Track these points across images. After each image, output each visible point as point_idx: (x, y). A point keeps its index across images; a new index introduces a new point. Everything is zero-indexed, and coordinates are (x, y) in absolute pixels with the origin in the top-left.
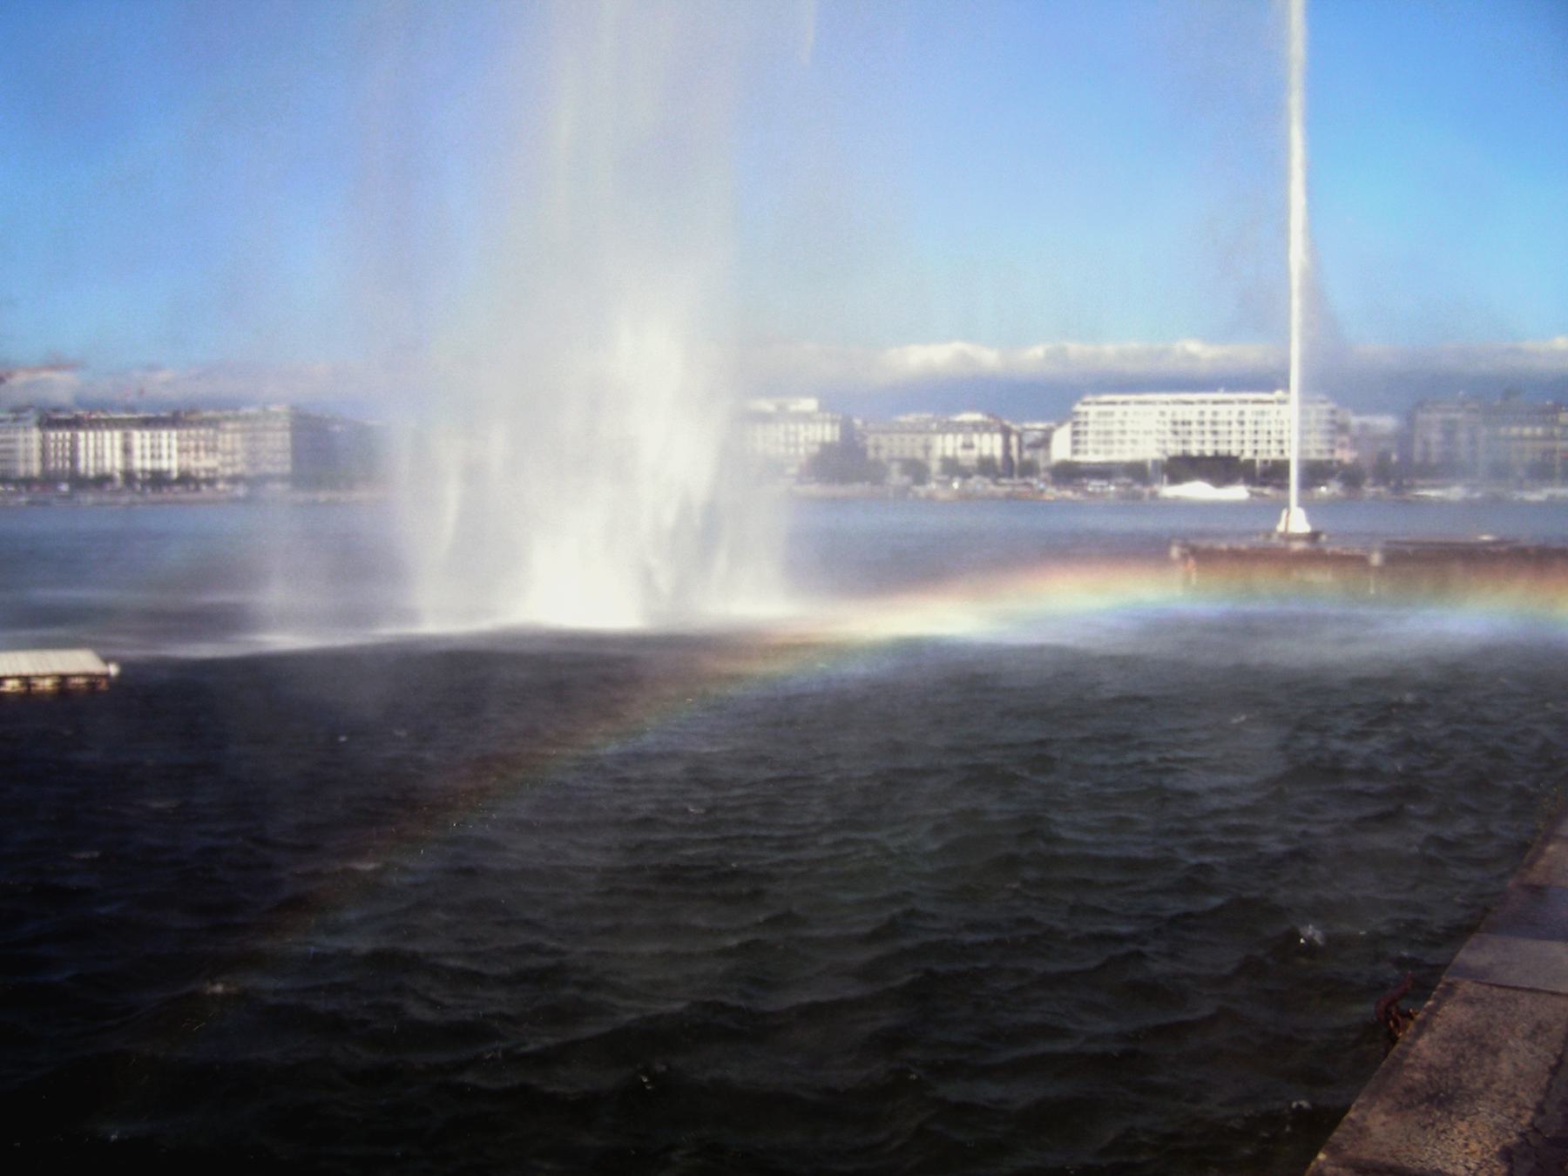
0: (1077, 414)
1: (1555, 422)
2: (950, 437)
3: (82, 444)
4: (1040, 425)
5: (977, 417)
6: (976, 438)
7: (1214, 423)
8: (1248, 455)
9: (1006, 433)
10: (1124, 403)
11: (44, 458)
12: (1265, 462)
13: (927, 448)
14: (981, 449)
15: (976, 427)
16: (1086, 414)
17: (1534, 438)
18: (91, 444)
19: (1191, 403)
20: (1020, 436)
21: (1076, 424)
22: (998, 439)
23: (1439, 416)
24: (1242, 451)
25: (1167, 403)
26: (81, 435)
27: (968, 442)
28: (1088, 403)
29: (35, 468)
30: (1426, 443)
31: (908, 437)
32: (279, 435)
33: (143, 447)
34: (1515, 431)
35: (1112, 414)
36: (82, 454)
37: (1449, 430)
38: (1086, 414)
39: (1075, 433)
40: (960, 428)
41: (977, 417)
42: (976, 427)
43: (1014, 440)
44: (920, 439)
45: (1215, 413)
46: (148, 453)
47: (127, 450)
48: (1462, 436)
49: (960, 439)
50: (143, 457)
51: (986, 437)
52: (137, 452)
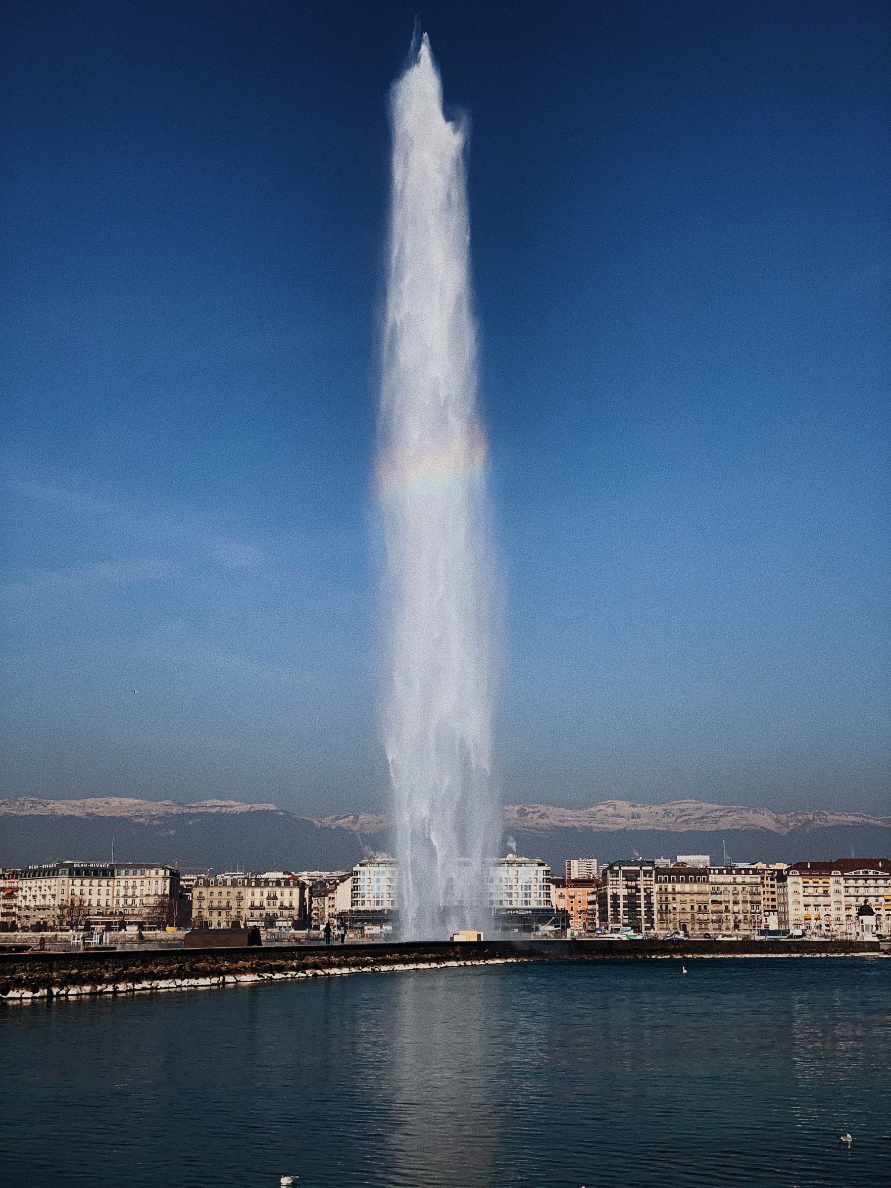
1: (705, 881)
2: (257, 891)
5: (280, 875)
6: (278, 891)
15: (278, 883)
16: (364, 873)
22: (296, 891)
38: (364, 873)
40: (267, 882)
42: (278, 883)
44: (234, 892)
49: (266, 891)
51: (287, 891)
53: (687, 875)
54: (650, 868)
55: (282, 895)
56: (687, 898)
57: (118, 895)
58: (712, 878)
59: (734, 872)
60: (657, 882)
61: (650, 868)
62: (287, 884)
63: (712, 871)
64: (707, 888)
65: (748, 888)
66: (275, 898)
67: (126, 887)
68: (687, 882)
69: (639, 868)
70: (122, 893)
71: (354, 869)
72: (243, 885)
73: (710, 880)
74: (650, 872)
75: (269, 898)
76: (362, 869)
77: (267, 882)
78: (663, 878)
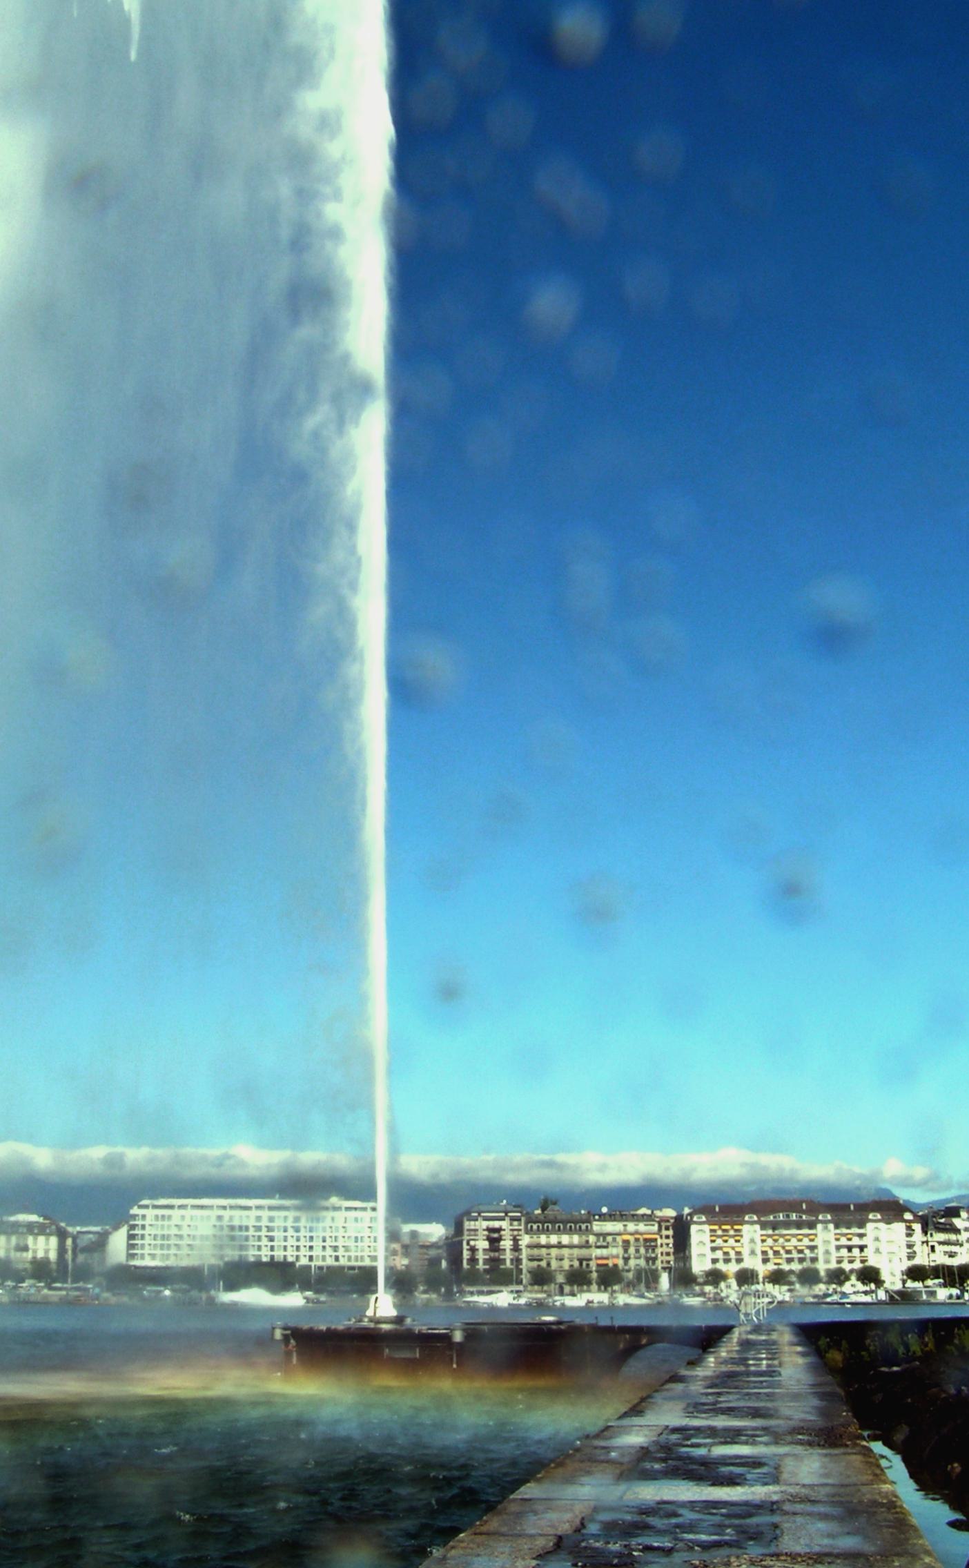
0: (134, 1217)
1: (588, 1231)
4: (97, 1229)
5: (34, 1218)
7: (269, 1229)
8: (304, 1261)
9: (62, 1235)
10: (180, 1207)
12: (321, 1268)
14: (35, 1251)
15: (31, 1228)
16: (144, 1217)
17: (571, 1246)
19: (210, 1207)
20: (75, 1239)
21: (133, 1227)
22: (54, 1241)
23: (485, 1224)
24: (298, 1257)
25: (224, 1208)
27: (22, 1244)
28: (146, 1207)
30: (473, 1250)
34: (554, 1239)
35: (170, 1217)
37: (494, 1239)
38: (144, 1217)
39: (131, 1237)
41: (34, 1218)
42: (31, 1228)
43: (69, 1242)
45: (271, 1219)
48: (507, 1244)
49: (14, 1240)
51: (41, 1239)
56: (566, 1252)
60: (527, 1233)
66: (26, 1249)
69: (503, 1214)
74: (518, 1219)
77: (16, 1225)
78: (535, 1227)
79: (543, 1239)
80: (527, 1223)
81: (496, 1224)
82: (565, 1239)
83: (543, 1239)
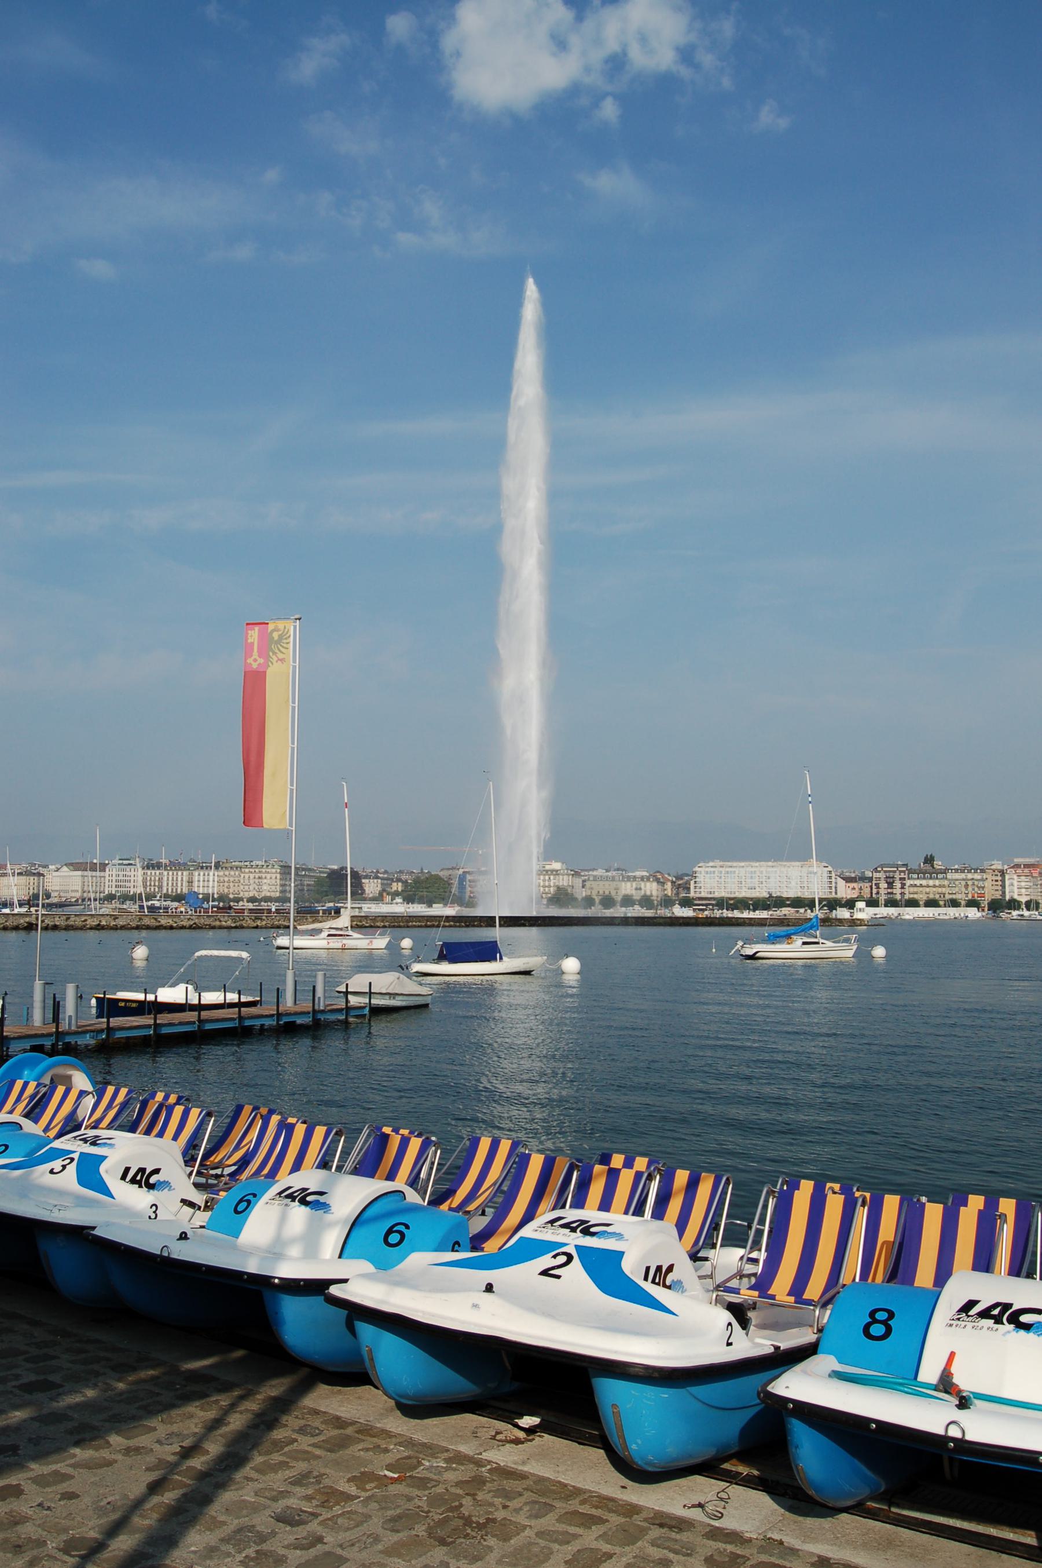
2: (629, 884)
3: (165, 878)
6: (643, 884)
11: (145, 887)
13: (617, 889)
15: (642, 878)
17: (935, 886)
18: (170, 879)
26: (165, 873)
29: (140, 890)
31: (607, 883)
32: (274, 876)
33: (199, 881)
34: (924, 882)
36: (165, 884)
38: (701, 872)
44: (614, 884)
46: (201, 884)
47: (190, 882)
49: (634, 884)
50: (198, 887)
51: (648, 884)
52: (196, 884)
53: (931, 874)
54: (905, 869)
55: (645, 887)
57: (539, 886)
58: (949, 876)
59: (966, 871)
61: (905, 869)
62: (648, 879)
63: (950, 871)
64: (946, 883)
65: (976, 883)
67: (544, 880)
68: (931, 878)
70: (542, 884)
71: (694, 870)
72: (619, 881)
73: (948, 877)
74: (904, 872)
75: (636, 889)
76: (700, 869)
79: (918, 882)
80: (909, 874)
81: (891, 874)
82: (931, 882)
83: (918, 882)
